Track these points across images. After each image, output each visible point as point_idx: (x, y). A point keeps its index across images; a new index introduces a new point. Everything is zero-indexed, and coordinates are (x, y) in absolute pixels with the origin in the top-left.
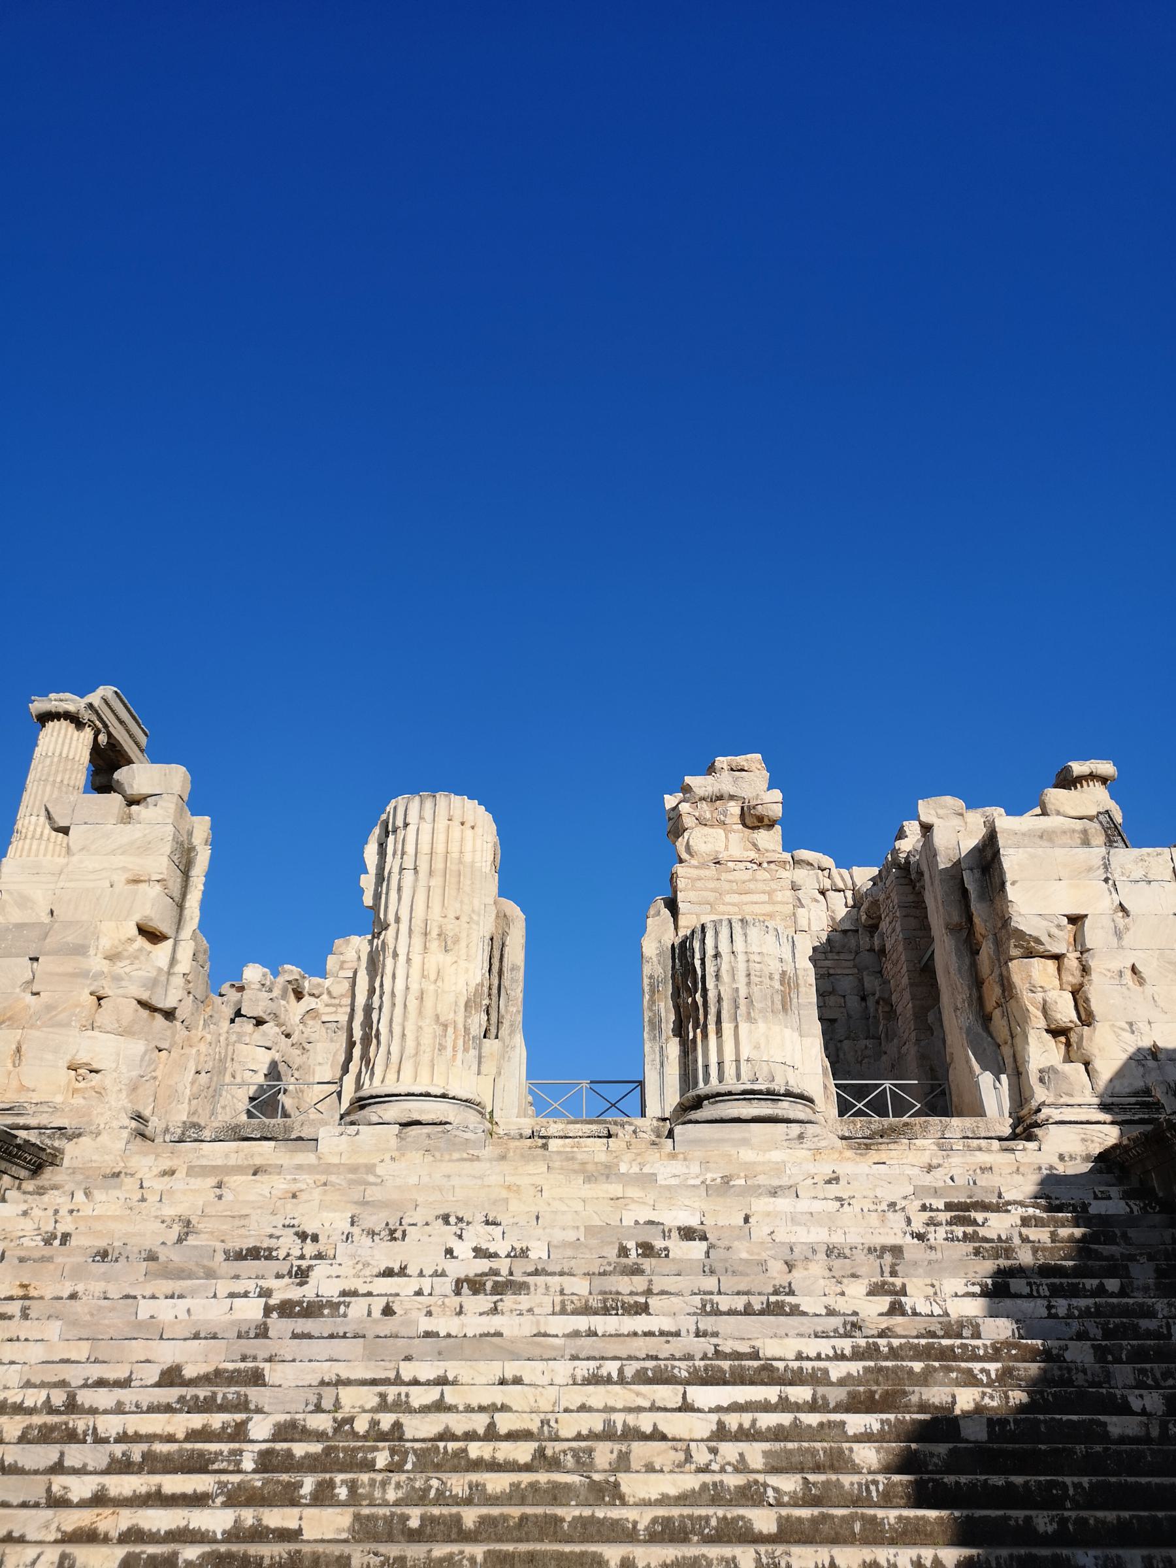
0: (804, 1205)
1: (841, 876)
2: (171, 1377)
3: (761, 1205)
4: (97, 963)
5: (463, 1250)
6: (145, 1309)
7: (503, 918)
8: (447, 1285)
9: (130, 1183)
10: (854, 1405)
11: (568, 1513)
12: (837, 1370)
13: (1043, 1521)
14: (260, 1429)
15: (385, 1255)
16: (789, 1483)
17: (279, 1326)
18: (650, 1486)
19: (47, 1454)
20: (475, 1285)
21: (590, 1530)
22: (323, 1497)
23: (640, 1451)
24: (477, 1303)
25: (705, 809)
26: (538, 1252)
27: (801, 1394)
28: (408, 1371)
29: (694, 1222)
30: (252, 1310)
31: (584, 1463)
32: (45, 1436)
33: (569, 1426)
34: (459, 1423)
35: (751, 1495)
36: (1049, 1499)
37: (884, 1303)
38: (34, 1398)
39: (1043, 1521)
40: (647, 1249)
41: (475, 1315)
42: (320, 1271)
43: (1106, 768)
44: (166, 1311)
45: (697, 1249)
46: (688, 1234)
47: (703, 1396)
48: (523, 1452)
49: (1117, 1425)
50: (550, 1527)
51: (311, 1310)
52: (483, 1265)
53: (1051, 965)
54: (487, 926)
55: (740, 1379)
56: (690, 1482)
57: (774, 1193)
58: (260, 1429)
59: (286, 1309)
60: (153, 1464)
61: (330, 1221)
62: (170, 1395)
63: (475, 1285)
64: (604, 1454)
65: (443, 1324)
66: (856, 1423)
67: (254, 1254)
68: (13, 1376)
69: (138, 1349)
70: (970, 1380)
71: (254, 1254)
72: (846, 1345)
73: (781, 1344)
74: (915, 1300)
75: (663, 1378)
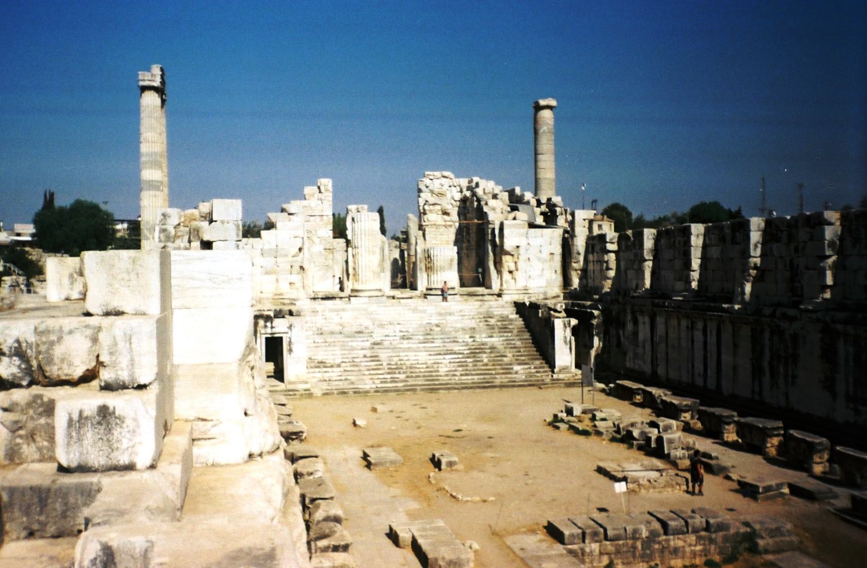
0: (456, 318)
1: (457, 181)
2: (365, 356)
3: (449, 318)
4: (290, 259)
5: (397, 331)
6: (350, 344)
7: (383, 242)
8: (398, 338)
9: (320, 314)
10: (468, 357)
11: (434, 374)
12: (466, 352)
13: (493, 372)
14: (385, 364)
15: (386, 332)
16: (460, 369)
17: (376, 347)
18: (443, 370)
19: (357, 369)
20: (403, 338)
21: (437, 376)
22: (399, 373)
23: (440, 365)
24: (405, 342)
25: (431, 207)
26: (411, 330)
27: (461, 356)
28: (401, 354)
29: (437, 322)
30: (368, 344)
31: (433, 367)
32: (353, 366)
33: (429, 362)
34: (413, 362)
35: (455, 371)
36: (495, 369)
37: (472, 340)
38: (347, 360)
39: (493, 372)
40: (431, 330)
41: (405, 344)
42: (374, 335)
43: (553, 103)
44: (354, 344)
45: (439, 329)
46: (437, 326)
47: (447, 357)
48: (424, 366)
49: (505, 359)
50: (431, 376)
51: (378, 344)
52: (402, 334)
53: (511, 257)
54: (380, 244)
55: (451, 354)
56: (447, 369)
57: (450, 314)
58: (385, 364)
59: (374, 344)
60: (373, 369)
61: (369, 323)
62: (365, 359)
63: (403, 338)
64: (436, 366)
65: (402, 346)
66: (469, 360)
67: (360, 332)
68: (340, 356)
69: (356, 352)
70: (485, 353)
71: (360, 332)
72: (466, 348)
73: (456, 348)
74: (478, 339)
75: (440, 354)
